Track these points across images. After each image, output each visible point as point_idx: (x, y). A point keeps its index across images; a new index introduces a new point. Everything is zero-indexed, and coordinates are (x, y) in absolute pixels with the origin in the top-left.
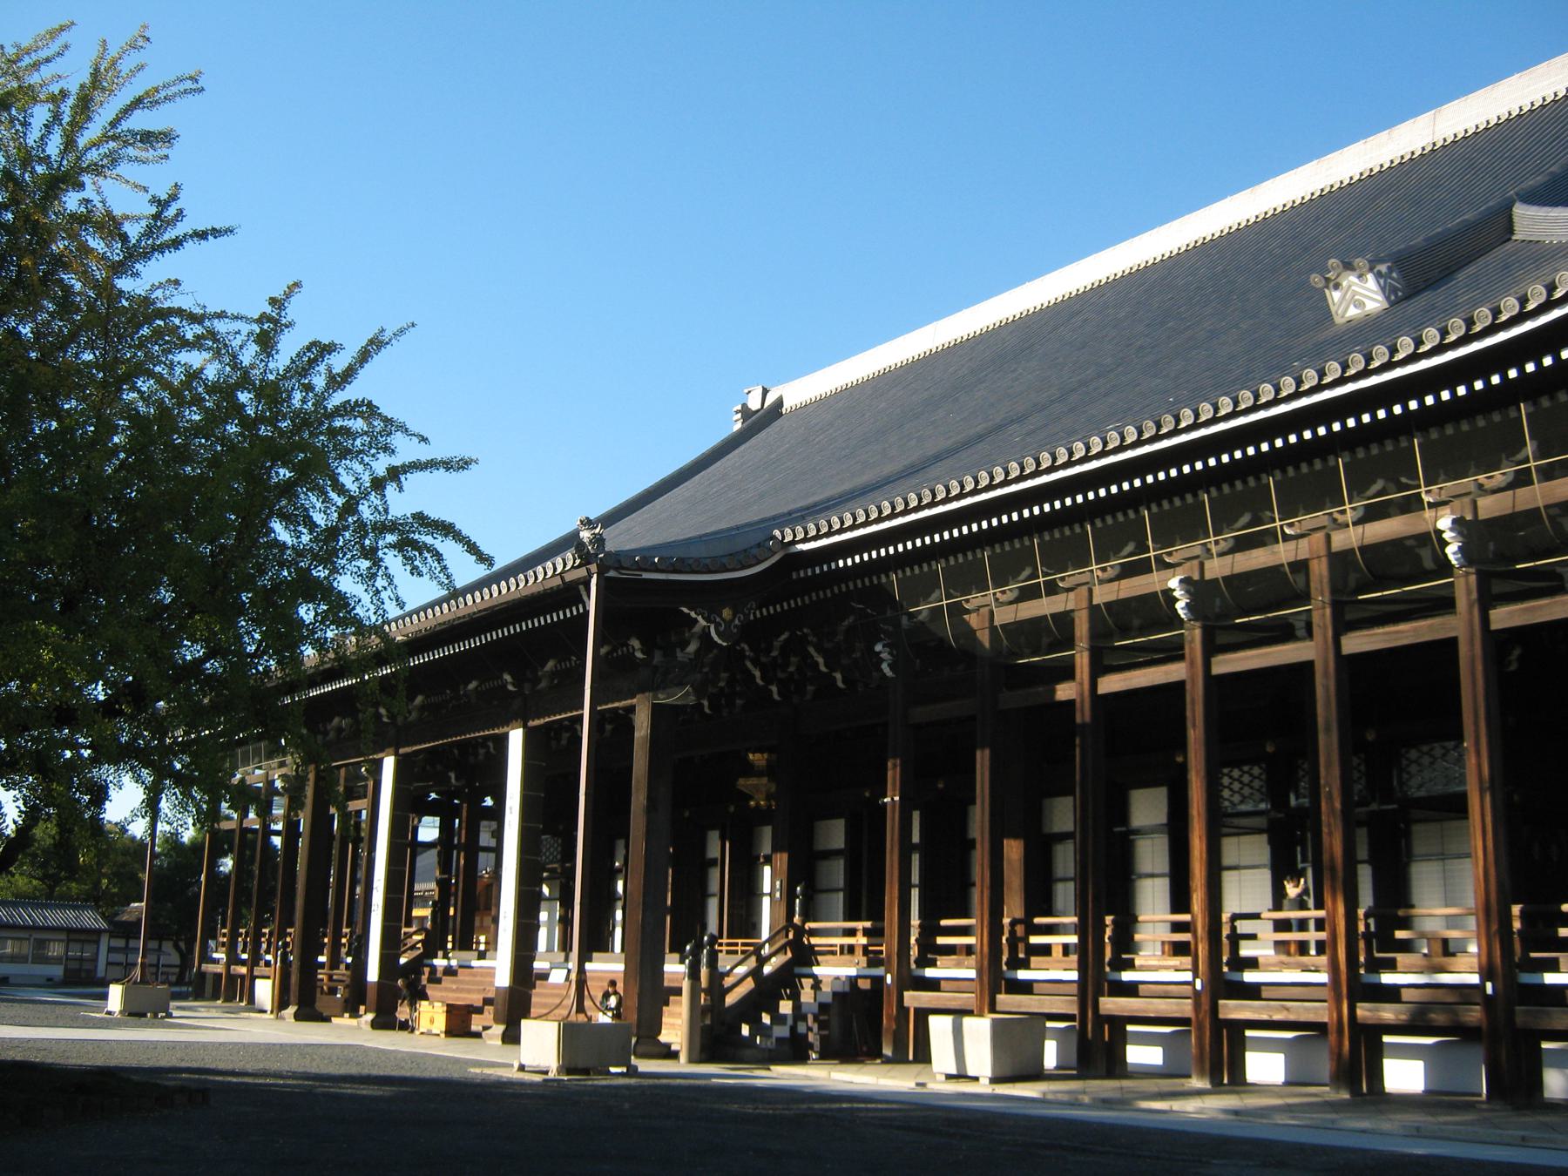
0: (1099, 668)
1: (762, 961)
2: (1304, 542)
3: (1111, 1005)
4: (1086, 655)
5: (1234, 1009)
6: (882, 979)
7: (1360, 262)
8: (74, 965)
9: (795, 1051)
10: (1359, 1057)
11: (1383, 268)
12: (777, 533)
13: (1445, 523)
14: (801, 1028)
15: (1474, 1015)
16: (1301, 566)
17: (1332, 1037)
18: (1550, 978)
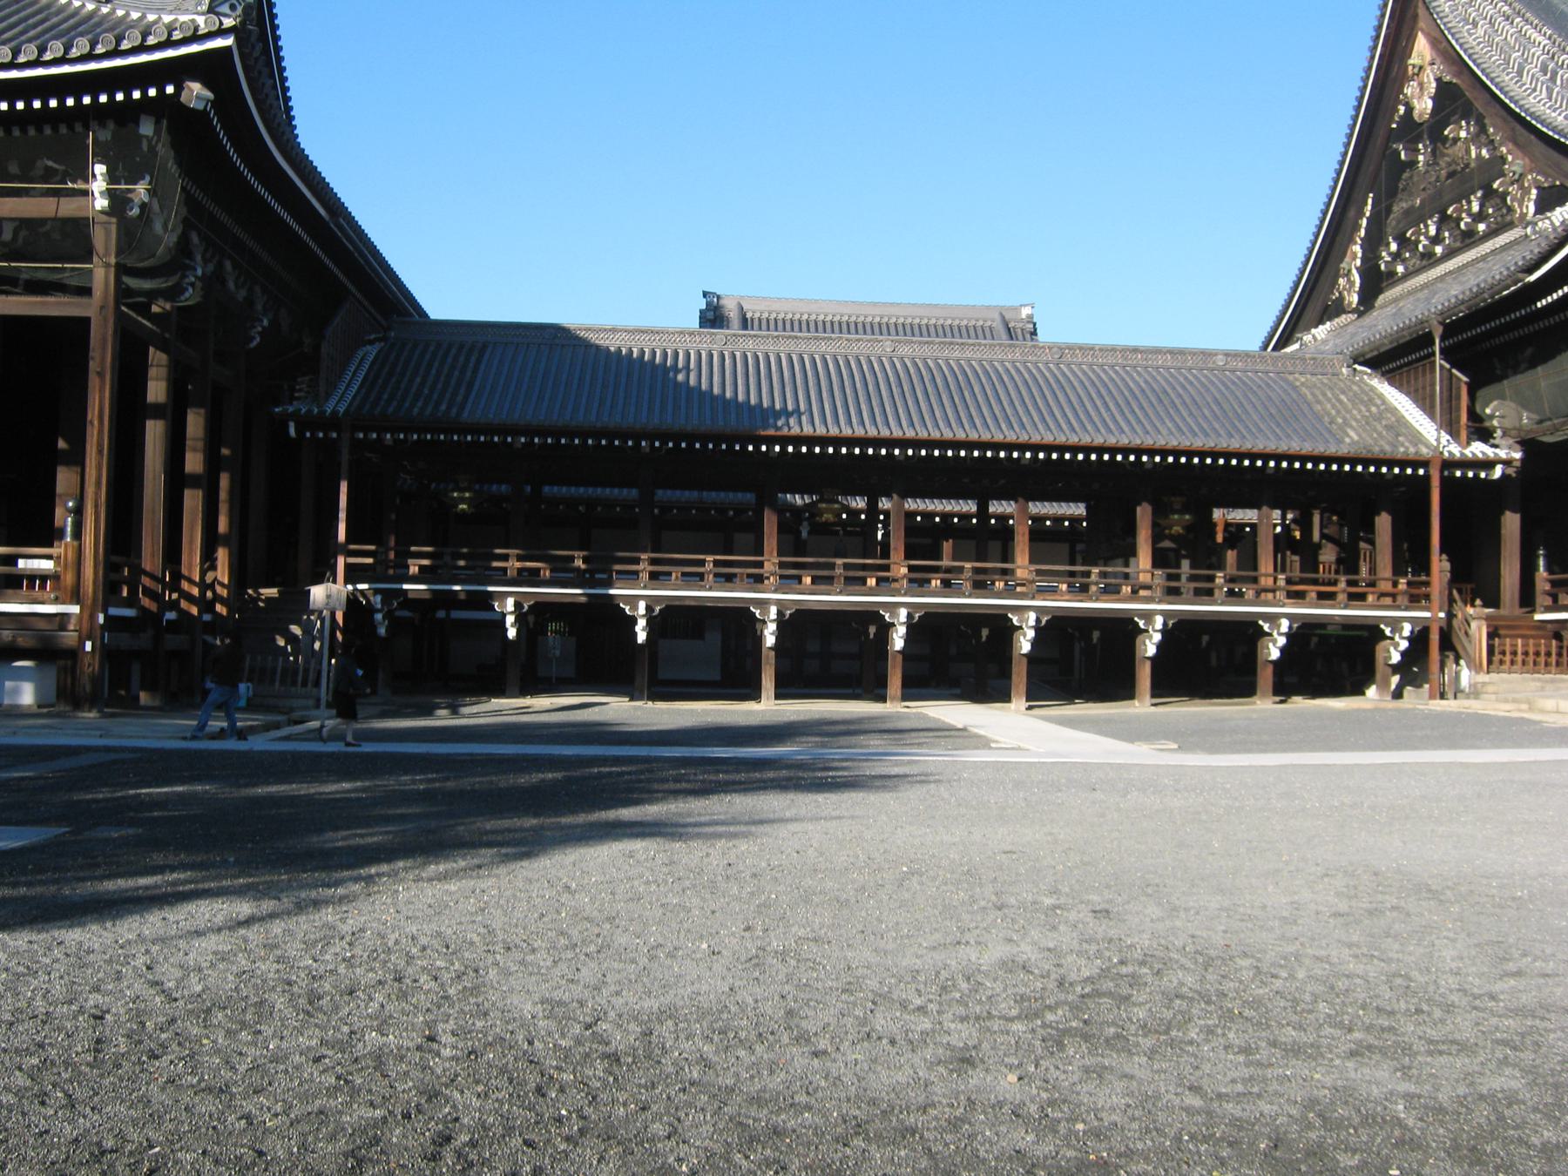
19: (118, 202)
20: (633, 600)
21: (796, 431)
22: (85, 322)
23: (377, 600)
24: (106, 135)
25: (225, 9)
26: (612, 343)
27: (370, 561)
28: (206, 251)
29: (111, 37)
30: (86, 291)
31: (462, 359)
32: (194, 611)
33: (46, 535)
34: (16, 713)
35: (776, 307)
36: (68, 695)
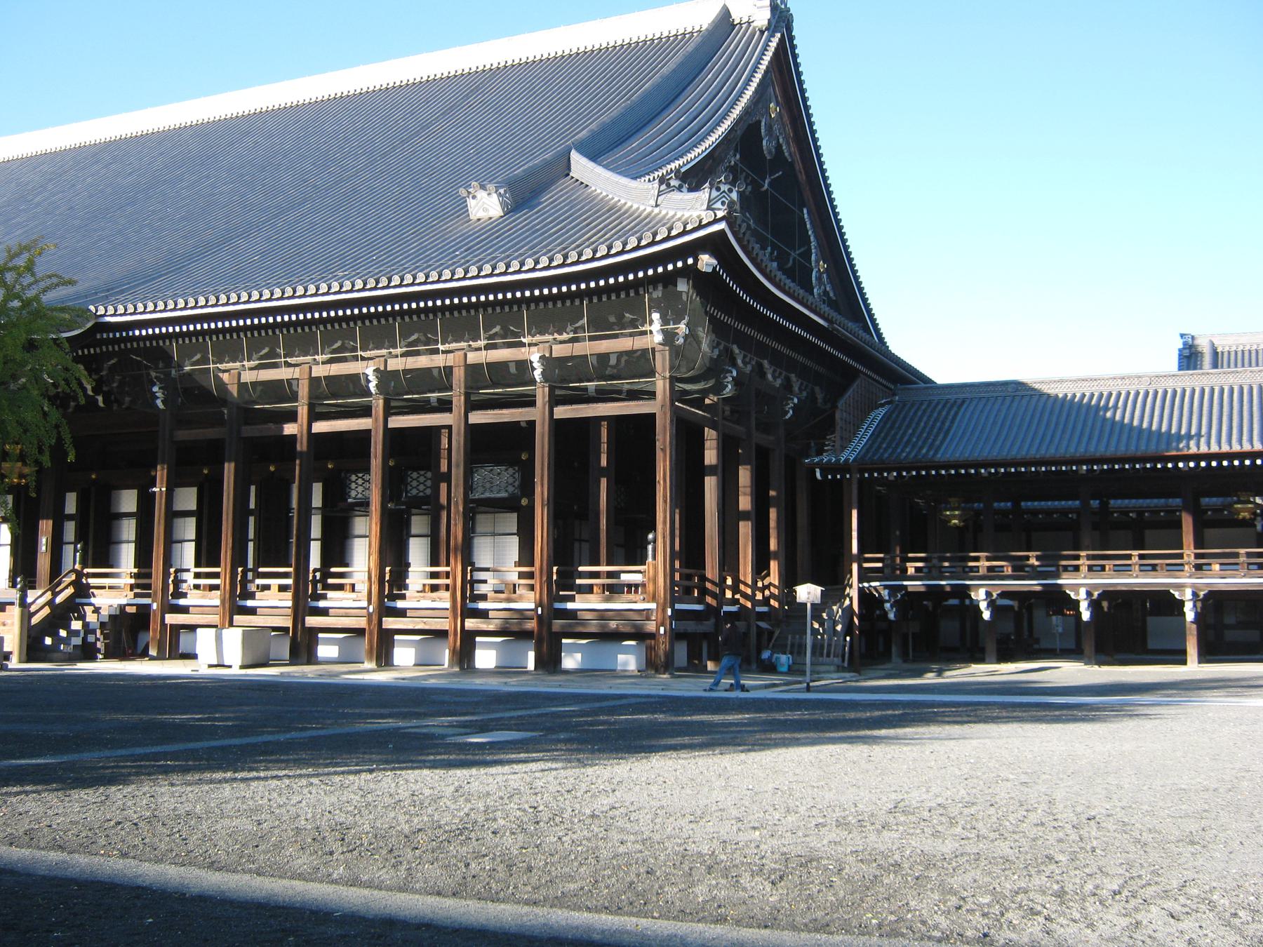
0: (314, 416)
1: (55, 595)
2: (450, 356)
3: (312, 621)
4: (306, 408)
5: (390, 623)
6: (149, 606)
7: (491, 187)
9: (88, 653)
10: (466, 647)
11: (502, 191)
12: (92, 308)
13: (535, 357)
14: (91, 638)
15: (532, 625)
16: (449, 370)
17: (451, 638)
18: (570, 606)
19: (669, 337)
20: (1076, 587)
21: (1193, 450)
22: (651, 417)
23: (885, 593)
24: (658, 293)
25: (718, 205)
26: (1059, 391)
27: (880, 565)
28: (745, 356)
29: (649, 234)
30: (652, 395)
31: (944, 413)
32: (749, 605)
33: (635, 555)
34: (624, 675)
35: (1243, 340)
36: (652, 665)
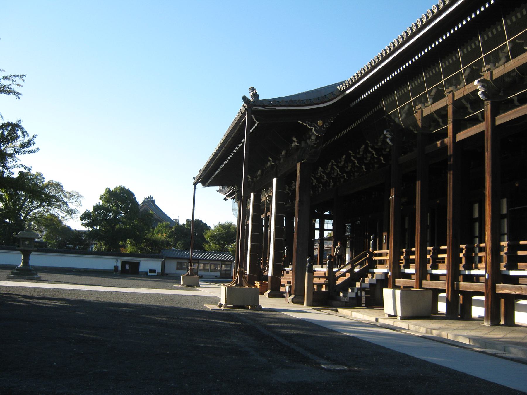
5: (503, 289)
8: (224, 272)
